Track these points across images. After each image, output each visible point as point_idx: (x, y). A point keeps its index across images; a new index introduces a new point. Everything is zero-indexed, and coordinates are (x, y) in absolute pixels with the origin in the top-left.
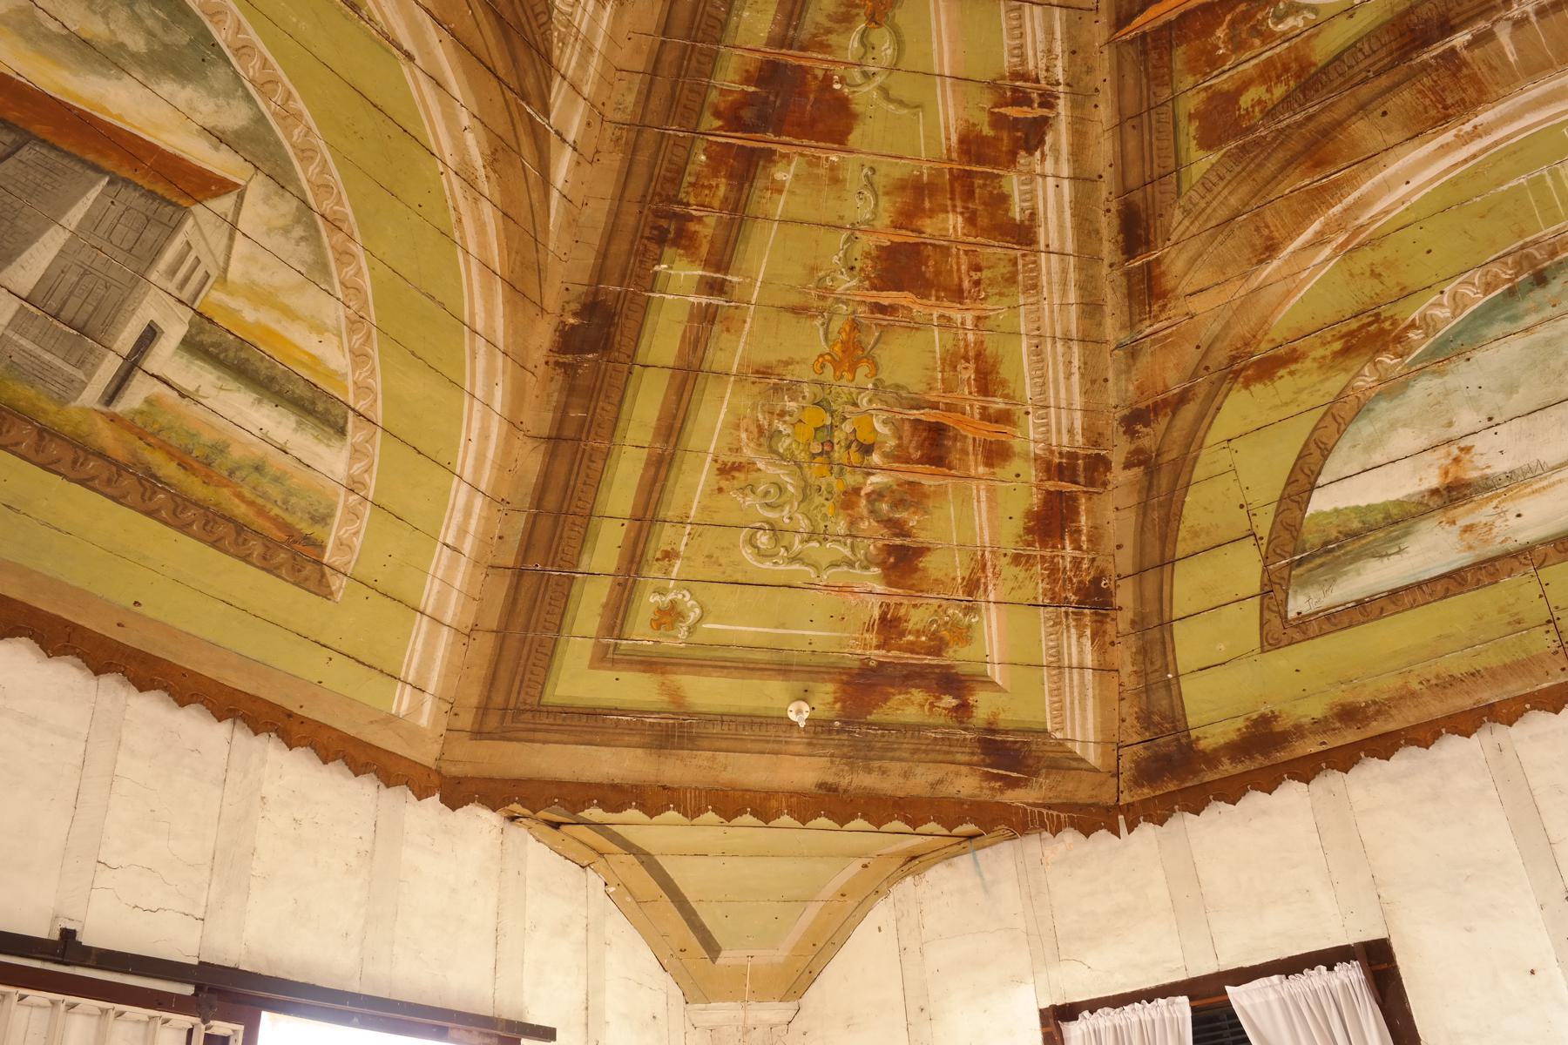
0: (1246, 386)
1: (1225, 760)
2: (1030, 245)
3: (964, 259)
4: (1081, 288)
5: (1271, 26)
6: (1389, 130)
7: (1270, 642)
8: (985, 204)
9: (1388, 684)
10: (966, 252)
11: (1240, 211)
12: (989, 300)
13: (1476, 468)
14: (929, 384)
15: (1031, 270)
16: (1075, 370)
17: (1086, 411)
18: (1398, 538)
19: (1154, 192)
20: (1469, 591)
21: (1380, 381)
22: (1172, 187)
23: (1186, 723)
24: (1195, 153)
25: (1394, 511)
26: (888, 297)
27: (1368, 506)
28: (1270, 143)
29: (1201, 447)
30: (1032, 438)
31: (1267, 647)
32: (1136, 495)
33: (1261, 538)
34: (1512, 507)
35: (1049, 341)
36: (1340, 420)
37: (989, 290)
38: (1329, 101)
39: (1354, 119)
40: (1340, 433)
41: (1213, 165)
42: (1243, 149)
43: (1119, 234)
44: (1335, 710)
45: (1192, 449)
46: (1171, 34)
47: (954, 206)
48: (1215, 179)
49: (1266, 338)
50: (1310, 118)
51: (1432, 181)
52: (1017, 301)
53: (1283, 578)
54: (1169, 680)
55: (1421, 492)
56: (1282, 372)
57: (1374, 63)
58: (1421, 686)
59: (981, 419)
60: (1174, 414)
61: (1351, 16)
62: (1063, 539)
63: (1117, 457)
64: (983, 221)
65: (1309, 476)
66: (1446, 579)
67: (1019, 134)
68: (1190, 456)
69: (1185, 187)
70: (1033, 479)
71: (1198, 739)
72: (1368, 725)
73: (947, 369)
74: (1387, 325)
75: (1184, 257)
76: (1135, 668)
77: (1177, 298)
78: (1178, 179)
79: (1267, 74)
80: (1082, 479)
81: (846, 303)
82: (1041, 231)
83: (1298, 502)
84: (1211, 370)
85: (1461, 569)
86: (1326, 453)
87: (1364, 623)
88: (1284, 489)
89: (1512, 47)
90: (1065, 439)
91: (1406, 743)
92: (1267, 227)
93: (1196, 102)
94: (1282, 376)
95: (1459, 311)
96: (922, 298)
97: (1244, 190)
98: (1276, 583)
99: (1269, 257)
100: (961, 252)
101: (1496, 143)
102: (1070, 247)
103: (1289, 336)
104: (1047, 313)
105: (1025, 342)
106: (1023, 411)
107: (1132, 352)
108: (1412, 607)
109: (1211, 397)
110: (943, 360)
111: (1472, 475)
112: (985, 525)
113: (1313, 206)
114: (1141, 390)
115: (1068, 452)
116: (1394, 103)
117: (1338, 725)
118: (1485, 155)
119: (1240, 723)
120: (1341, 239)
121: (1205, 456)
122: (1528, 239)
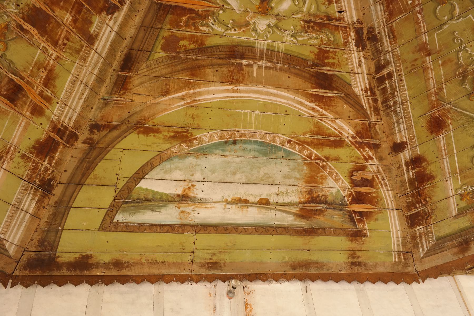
0: (138, 133)
1: (65, 269)
2: (91, 45)
3: (64, 32)
4: (100, 71)
5: (199, 26)
6: (216, 76)
7: (103, 228)
8: (82, 19)
9: (135, 257)
10: (67, 31)
11: (163, 76)
12: (66, 54)
13: (193, 193)
14: (25, 69)
15: (86, 53)
16: (83, 98)
17: (79, 115)
18: (161, 206)
19: (140, 54)
20: (174, 233)
21: (179, 152)
22: (147, 56)
23: (57, 249)
24: (159, 50)
25: (164, 197)
26: (26, 26)
27: (157, 192)
28: (182, 60)
29: (113, 147)
30: (54, 113)
31: (101, 229)
32: (82, 154)
33: (118, 189)
34: (198, 210)
35: (80, 82)
36: (162, 159)
37: (68, 50)
38: (204, 58)
39: (208, 67)
40: (160, 163)
41: (162, 57)
42: (174, 57)
43: (122, 61)
44: (113, 261)
45: (110, 147)
46: (170, 9)
47: (71, 12)
48: (161, 61)
49: (153, 121)
50: (197, 60)
52: (76, 60)
53: (118, 206)
54: (59, 230)
55: (174, 194)
56: (152, 134)
57: (221, 55)
58: (145, 261)
59: (39, 94)
60: (110, 132)
61: (221, 38)
62: (46, 157)
63: (82, 137)
64: (79, 25)
65: (143, 173)
66: (169, 227)
67: (107, 5)
68: (108, 149)
69: (151, 58)
70: (47, 128)
71: (58, 257)
72: (122, 270)
73: (36, 67)
74: (189, 135)
75: (140, 80)
76: (48, 221)
77: (130, 93)
78: (150, 54)
79: (192, 39)
80: (65, 139)
81: (8, 16)
82: (97, 42)
83: (136, 181)
84: (130, 122)
85: (175, 225)
86: (152, 168)
87: (137, 232)
88: (133, 175)
90: (66, 121)
91: (132, 281)
92: (169, 85)
93: (167, 34)
94: (151, 136)
95: (210, 141)
96: (40, 35)
97: (168, 70)
98: (115, 207)
99: (165, 95)
100: (65, 30)
101: (241, 97)
102: (104, 55)
103: (159, 123)
104: (84, 72)
105: (70, 77)
106: (57, 101)
107: (106, 103)
108: (155, 232)
109: (125, 132)
110: (36, 63)
111: (191, 195)
112: (18, 136)
113: (185, 87)
114: (103, 117)
115: (65, 126)
116: (221, 69)
117: (112, 267)
119: (77, 256)
120: (189, 101)
121: (113, 151)
122: (237, 129)
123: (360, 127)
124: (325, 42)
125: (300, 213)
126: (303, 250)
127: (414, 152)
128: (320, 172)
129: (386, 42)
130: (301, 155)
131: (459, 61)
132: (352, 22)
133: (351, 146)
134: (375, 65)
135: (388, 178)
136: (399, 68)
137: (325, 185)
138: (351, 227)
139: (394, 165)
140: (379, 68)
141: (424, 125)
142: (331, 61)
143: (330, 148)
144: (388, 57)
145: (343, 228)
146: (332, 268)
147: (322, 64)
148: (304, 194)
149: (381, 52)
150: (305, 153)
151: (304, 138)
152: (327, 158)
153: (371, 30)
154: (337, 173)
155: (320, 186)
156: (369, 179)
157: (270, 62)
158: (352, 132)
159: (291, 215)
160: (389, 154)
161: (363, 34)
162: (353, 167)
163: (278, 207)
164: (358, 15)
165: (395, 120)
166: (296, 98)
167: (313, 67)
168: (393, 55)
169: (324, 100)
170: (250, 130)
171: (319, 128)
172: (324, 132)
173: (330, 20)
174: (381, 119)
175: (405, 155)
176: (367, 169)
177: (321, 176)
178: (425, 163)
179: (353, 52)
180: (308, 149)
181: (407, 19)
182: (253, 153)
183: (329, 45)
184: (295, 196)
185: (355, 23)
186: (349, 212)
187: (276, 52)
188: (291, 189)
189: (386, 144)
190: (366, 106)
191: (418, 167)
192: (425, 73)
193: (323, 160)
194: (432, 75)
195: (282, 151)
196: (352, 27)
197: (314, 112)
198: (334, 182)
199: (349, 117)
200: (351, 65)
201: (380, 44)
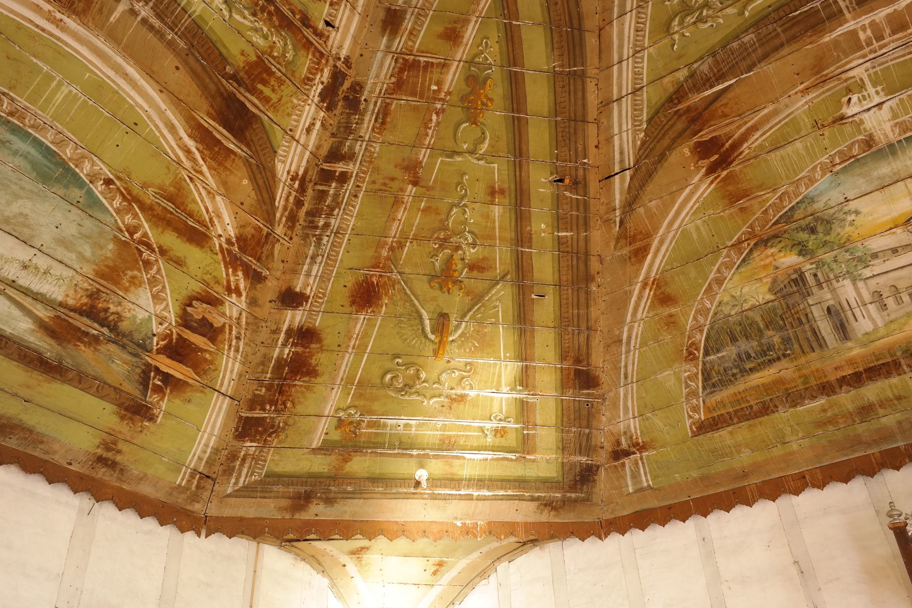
51: (12, 11)
89: (118, 15)
101: (58, 39)
118: (48, 37)
122: (11, 94)
123: (249, 231)
124: (275, 54)
125: (51, 323)
126: (15, 395)
127: (310, 318)
128: (135, 267)
129: (369, 121)
130: (117, 218)
131: (447, 219)
132: (336, 54)
133: (217, 254)
134: (332, 147)
135: (247, 341)
136: (363, 175)
137: (131, 297)
138: (137, 393)
139: (269, 324)
140: (335, 155)
141: (349, 285)
142: (267, 91)
143: (177, 237)
144: (357, 147)
145: (119, 389)
146: (55, 452)
147: (250, 87)
148: (81, 293)
149: (352, 133)
150: (126, 220)
151: (141, 193)
152: (163, 252)
153: (358, 88)
154: (164, 287)
155: (120, 293)
156: (215, 325)
157: (158, 16)
158: (232, 232)
159: (30, 318)
160: (270, 302)
161: (342, 84)
162: (199, 291)
163: (10, 292)
164: (352, 50)
165: (311, 252)
166: (168, 113)
167: (231, 81)
168: (366, 149)
169: (216, 149)
170: (40, 112)
171: (179, 190)
172: (183, 204)
173: (304, 25)
174: (291, 239)
175: (295, 317)
176: (220, 307)
177: (133, 277)
178: (318, 346)
179: (310, 102)
180: (136, 216)
181: (416, 109)
182: (19, 161)
183: (279, 63)
184: (59, 286)
185: (339, 59)
186: (148, 365)
187: (180, 8)
188: (58, 269)
189: (275, 282)
190: (279, 202)
191: (303, 346)
192: (395, 207)
193: (153, 251)
194: (402, 217)
195: (84, 191)
196: (331, 62)
197: (187, 158)
198: (151, 300)
199: (242, 204)
200: (295, 120)
201: (358, 119)
